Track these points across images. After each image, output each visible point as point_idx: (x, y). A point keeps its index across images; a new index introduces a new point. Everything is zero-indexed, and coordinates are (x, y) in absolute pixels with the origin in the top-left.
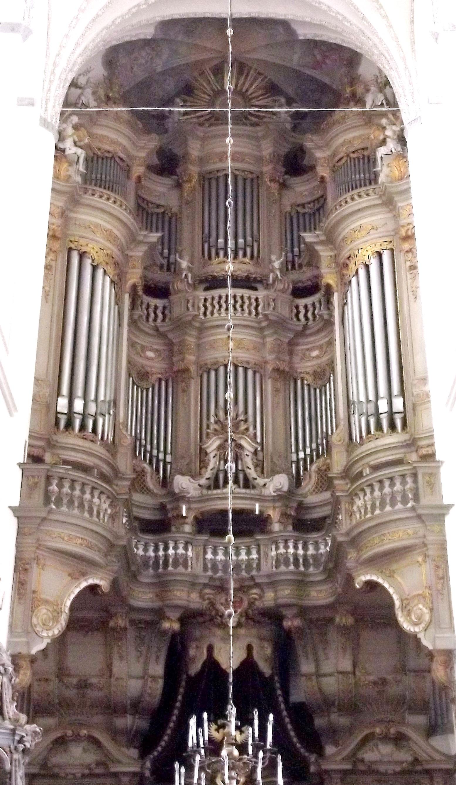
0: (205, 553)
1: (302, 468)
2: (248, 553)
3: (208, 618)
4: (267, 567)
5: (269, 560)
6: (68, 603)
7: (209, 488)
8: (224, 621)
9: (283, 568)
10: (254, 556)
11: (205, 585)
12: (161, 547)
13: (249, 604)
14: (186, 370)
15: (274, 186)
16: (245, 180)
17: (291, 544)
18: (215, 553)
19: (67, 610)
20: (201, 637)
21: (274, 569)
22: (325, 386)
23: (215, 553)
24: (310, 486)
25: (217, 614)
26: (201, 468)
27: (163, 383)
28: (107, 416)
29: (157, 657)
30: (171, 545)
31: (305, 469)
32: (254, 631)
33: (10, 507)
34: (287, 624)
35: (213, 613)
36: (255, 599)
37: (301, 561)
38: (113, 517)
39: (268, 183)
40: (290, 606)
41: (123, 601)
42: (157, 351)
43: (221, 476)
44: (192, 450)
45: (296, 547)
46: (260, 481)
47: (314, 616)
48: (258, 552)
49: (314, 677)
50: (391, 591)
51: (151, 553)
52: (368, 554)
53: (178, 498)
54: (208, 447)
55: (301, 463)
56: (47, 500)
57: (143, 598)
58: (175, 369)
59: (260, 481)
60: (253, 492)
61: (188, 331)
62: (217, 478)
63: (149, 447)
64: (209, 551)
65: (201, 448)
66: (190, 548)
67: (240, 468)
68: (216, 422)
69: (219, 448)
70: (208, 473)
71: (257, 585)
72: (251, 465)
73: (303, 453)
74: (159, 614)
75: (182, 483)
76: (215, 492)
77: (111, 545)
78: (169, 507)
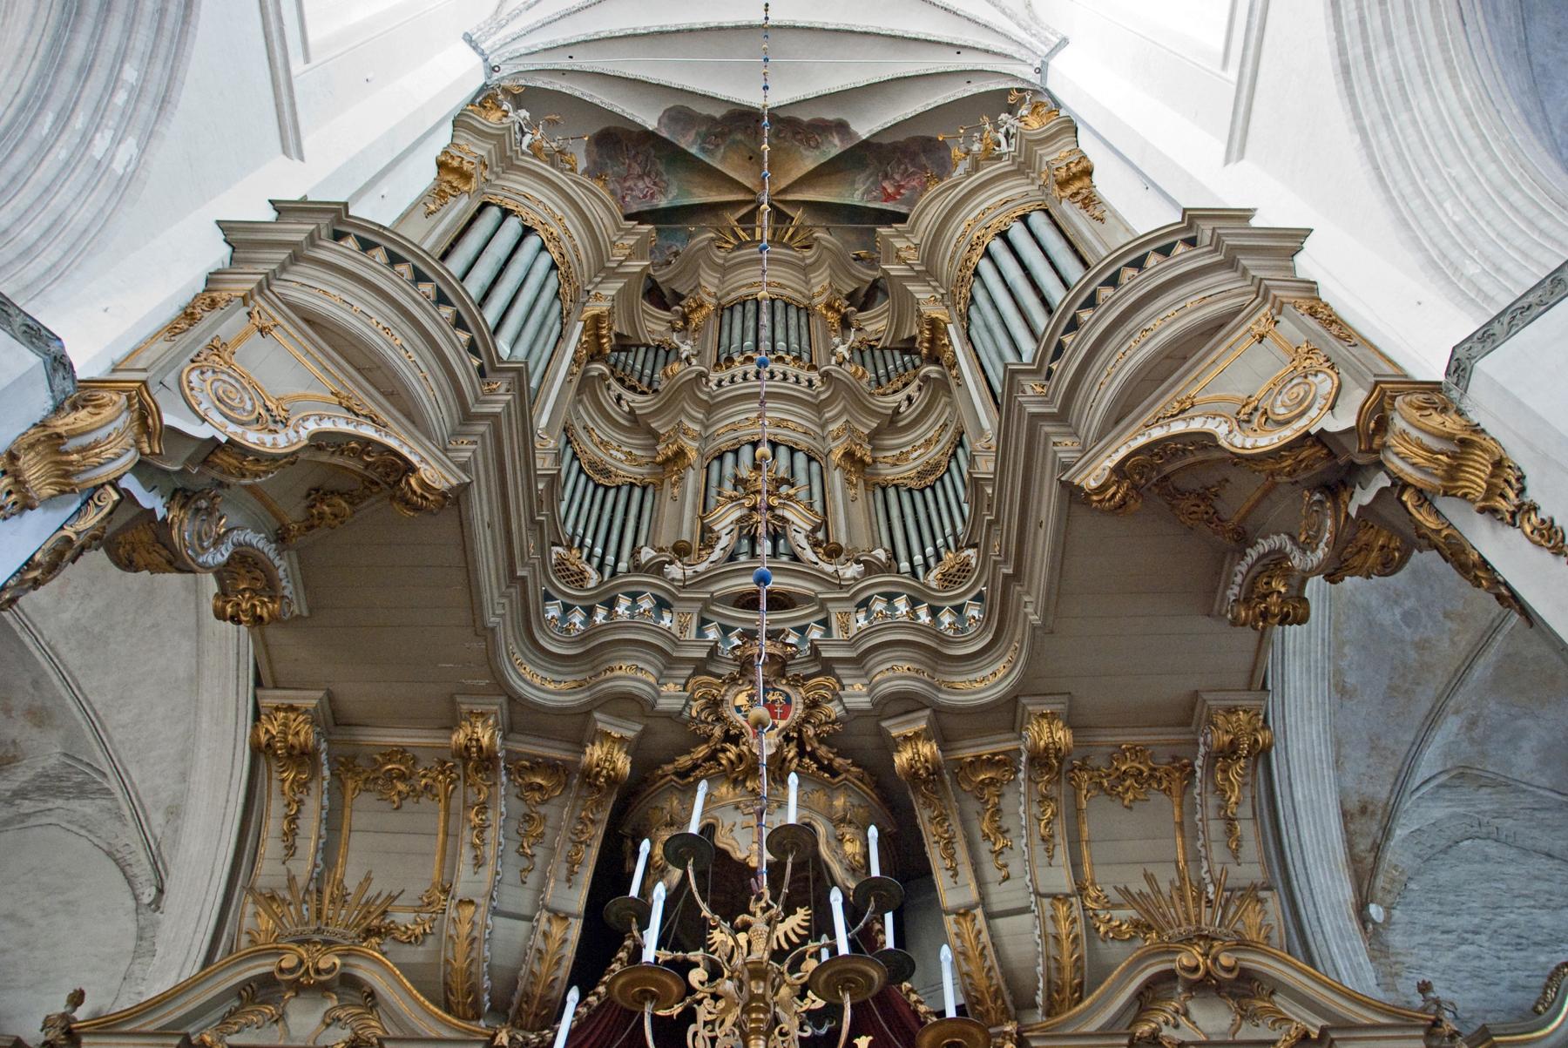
3: (702, 751)
6: (312, 426)
8: (745, 748)
11: (701, 667)
13: (807, 707)
14: (680, 454)
16: (787, 305)
19: (304, 434)
22: (941, 479)
27: (637, 493)
29: (573, 864)
33: (218, 222)
34: (902, 759)
35: (718, 731)
47: (967, 754)
49: (979, 912)
67: (782, 549)
71: (827, 667)
77: (467, 417)
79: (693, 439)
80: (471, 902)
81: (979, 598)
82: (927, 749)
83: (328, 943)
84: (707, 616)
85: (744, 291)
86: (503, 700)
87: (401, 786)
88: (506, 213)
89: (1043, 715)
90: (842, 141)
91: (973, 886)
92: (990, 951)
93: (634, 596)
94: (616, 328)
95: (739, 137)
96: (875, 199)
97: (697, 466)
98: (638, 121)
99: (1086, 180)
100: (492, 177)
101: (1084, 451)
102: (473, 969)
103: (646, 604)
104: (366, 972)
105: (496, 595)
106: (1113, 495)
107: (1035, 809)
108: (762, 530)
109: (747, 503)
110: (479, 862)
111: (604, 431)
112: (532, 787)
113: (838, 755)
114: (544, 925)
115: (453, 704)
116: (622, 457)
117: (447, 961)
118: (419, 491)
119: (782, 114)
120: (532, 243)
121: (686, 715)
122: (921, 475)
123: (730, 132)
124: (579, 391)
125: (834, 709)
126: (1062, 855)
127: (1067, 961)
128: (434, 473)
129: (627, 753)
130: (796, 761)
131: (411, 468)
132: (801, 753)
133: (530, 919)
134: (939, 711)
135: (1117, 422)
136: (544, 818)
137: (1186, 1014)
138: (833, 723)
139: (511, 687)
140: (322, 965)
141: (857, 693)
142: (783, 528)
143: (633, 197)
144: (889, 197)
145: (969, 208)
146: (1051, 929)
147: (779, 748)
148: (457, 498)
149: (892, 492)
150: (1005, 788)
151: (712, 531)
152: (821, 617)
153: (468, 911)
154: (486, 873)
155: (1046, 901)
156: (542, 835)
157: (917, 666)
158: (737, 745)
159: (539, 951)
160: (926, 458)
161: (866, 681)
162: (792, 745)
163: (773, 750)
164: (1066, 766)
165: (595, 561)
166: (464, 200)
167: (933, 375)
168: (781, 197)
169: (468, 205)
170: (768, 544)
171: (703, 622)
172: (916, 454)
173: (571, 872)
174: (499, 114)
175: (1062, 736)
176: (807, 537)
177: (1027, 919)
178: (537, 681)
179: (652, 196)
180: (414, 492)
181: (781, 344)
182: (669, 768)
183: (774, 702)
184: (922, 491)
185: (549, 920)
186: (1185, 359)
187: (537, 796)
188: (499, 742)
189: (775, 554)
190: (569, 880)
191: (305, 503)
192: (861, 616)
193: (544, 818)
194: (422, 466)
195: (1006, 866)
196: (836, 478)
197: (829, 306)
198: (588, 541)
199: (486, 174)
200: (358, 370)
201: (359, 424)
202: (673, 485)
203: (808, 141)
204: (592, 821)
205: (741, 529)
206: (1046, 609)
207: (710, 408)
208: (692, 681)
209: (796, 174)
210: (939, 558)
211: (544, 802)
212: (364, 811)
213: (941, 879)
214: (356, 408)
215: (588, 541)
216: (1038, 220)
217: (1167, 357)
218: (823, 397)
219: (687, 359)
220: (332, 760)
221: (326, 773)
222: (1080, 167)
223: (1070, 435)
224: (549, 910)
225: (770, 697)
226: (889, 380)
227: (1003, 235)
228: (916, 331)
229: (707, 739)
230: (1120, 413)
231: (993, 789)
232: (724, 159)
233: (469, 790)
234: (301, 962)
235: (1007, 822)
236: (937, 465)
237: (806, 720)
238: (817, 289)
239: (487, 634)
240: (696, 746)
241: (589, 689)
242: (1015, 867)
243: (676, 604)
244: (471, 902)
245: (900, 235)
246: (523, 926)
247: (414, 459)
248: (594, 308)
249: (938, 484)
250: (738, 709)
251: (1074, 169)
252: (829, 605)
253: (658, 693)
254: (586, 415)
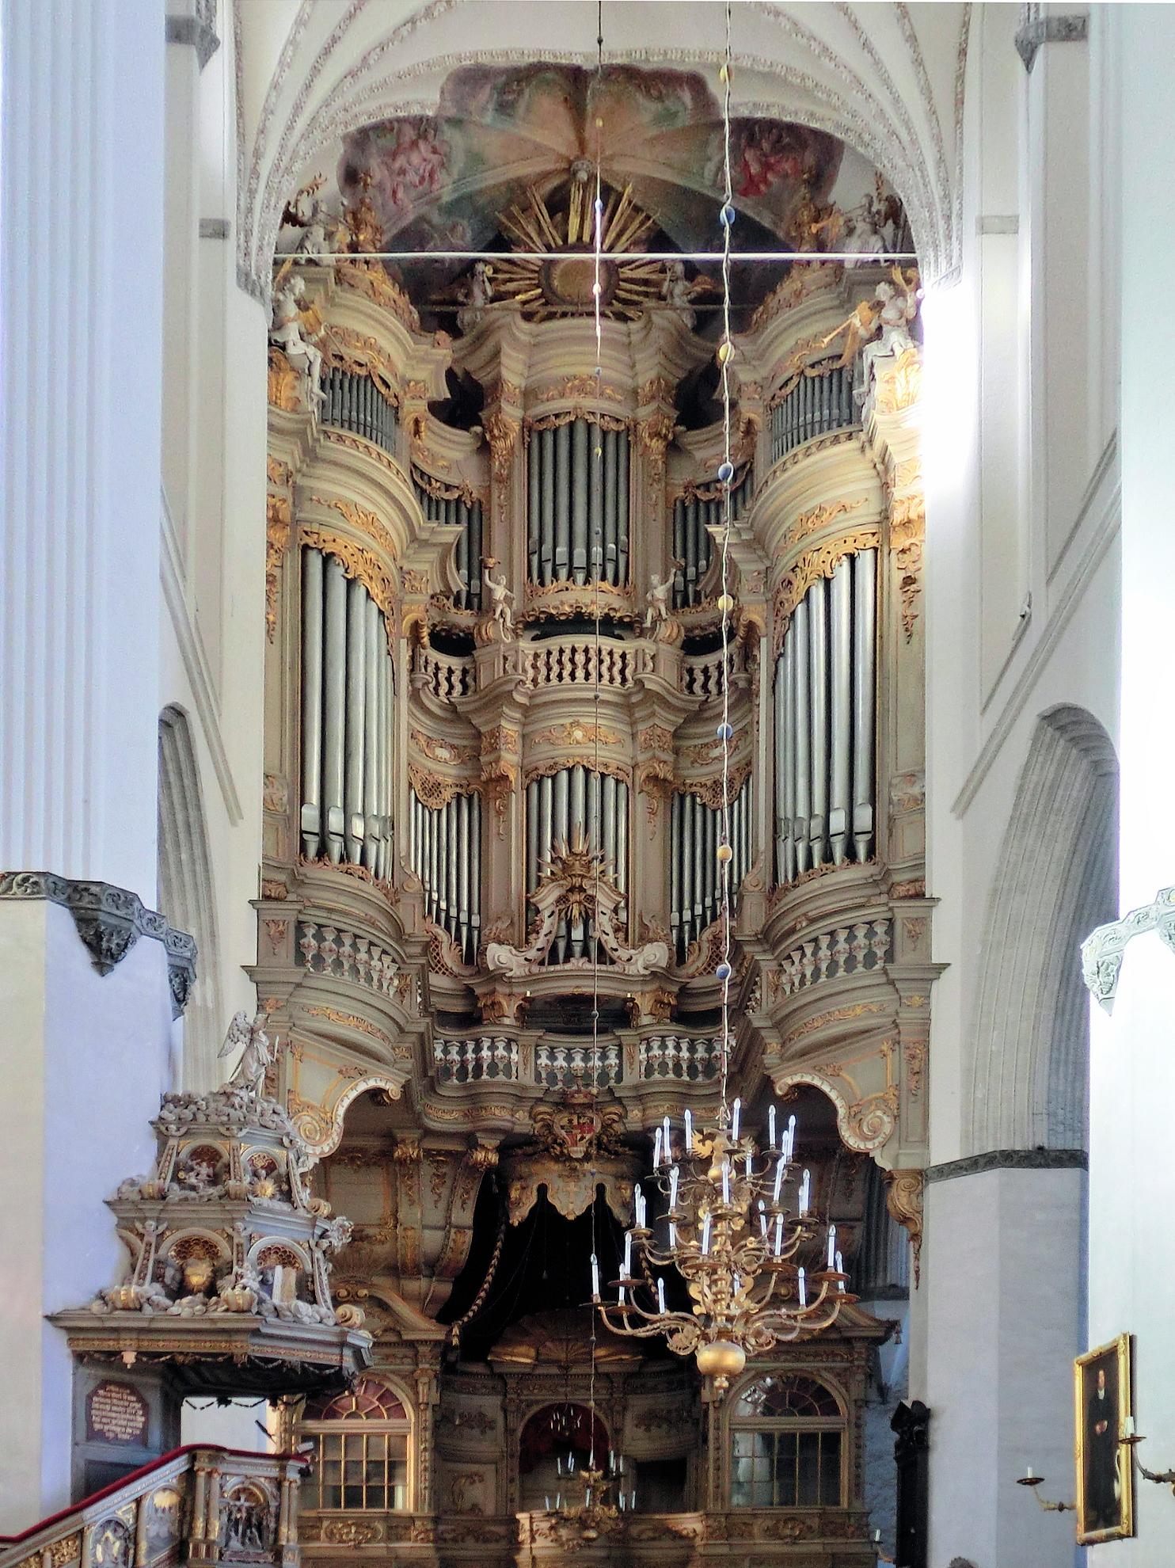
0: (537, 1056)
1: (686, 936)
2: (604, 1057)
3: (541, 1147)
4: (631, 1077)
5: (636, 1066)
7: (542, 963)
9: (657, 1076)
10: (613, 1060)
12: (471, 1046)
17: (670, 1044)
18: (552, 1057)
20: (531, 1175)
21: (643, 1079)
23: (552, 1057)
24: (699, 964)
25: (555, 1142)
26: (528, 934)
28: (383, 842)
30: (486, 1043)
31: (693, 938)
32: (611, 1168)
36: (614, 1121)
37: (685, 1067)
38: (401, 992)
41: (417, 1122)
43: (562, 944)
45: (678, 1048)
46: (623, 954)
48: (620, 1056)
50: (833, 1095)
51: (455, 1056)
52: (799, 1044)
53: (497, 977)
54: (542, 901)
55: (687, 927)
56: (300, 958)
57: (445, 1116)
59: (623, 954)
60: (611, 968)
62: (554, 948)
64: (544, 1054)
65: (528, 900)
66: (514, 1048)
68: (553, 861)
69: (559, 900)
70: (540, 941)
71: (619, 1101)
72: (609, 930)
74: (470, 1140)
75: (498, 955)
76: (552, 968)
78: (478, 991)
84: (540, 1042)
108: (576, 912)
182: (520, 1152)
205: (560, 911)
250: (562, 1127)
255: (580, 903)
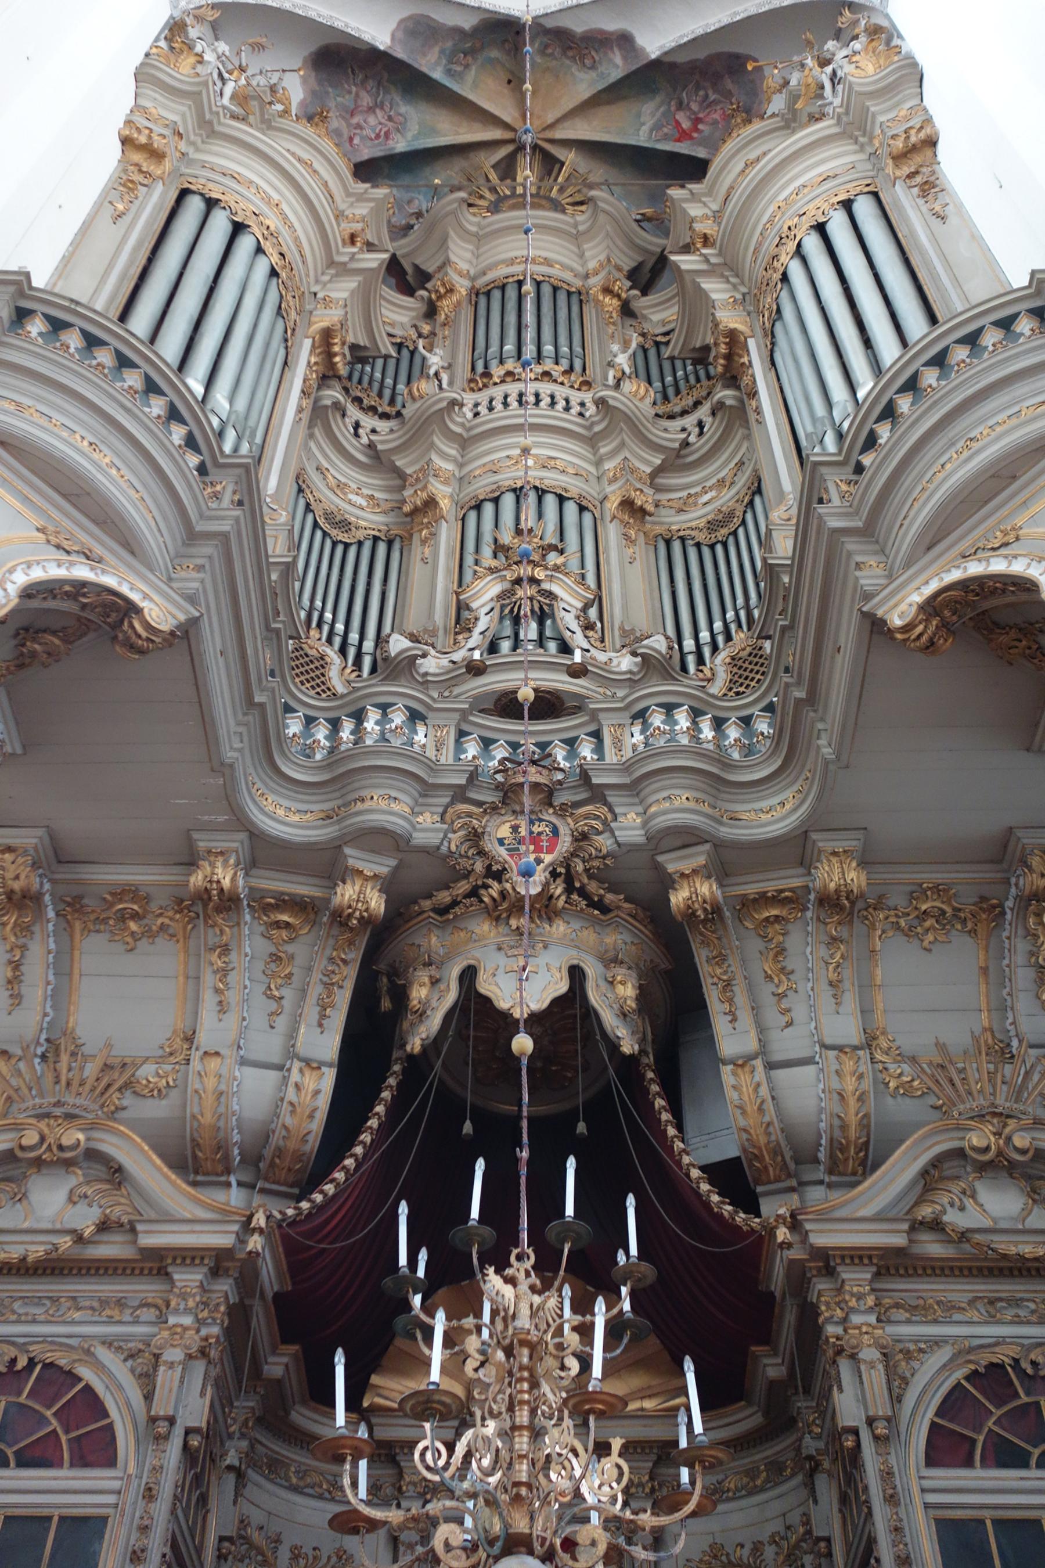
3: (463, 887)
6: (20, 579)
8: (508, 886)
11: (459, 794)
14: (431, 503)
15: (611, 304)
16: (555, 289)
19: (13, 590)
22: (735, 533)
27: (382, 548)
29: (324, 1008)
32: (589, 936)
34: (678, 898)
35: (479, 867)
39: (601, 297)
40: (686, 838)
42: (372, 497)
44: (439, 617)
47: (751, 889)
49: (758, 1063)
58: (407, 508)
61: (435, 439)
63: (340, 627)
67: (548, 633)
71: (598, 794)
73: (692, 642)
79: (446, 482)
80: (217, 1054)
81: (770, 708)
82: (706, 889)
83: (70, 1117)
84: (466, 727)
85: (502, 271)
86: (243, 836)
87: (133, 926)
88: (211, 203)
89: (835, 854)
90: (625, 58)
91: (753, 1034)
92: (769, 1105)
93: (384, 708)
94: (350, 339)
95: (495, 53)
96: (666, 138)
97: (451, 518)
98: (366, 37)
99: (929, 152)
100: (191, 151)
101: (891, 577)
102: (221, 1124)
103: (398, 718)
104: (111, 1146)
105: (232, 722)
106: (920, 635)
107: (823, 952)
109: (509, 575)
110: (222, 1008)
111: (342, 471)
112: (278, 925)
113: (609, 890)
114: (295, 1076)
115: (191, 844)
116: (360, 502)
117: (193, 1117)
118: (144, 634)
119: (549, 24)
120: (245, 244)
121: (444, 849)
122: (712, 526)
123: (482, 48)
124: (311, 426)
125: (604, 842)
126: (850, 1001)
127: (853, 1120)
128: (158, 610)
129: (380, 891)
130: (563, 898)
131: (131, 609)
132: (569, 889)
133: (280, 1068)
134: (719, 846)
135: (929, 549)
136: (291, 957)
137: (973, 1196)
138: (604, 857)
139: (253, 823)
140: (66, 1141)
141: (630, 825)
142: (551, 606)
143: (362, 138)
144: (683, 136)
145: (782, 178)
146: (835, 1084)
147: (546, 885)
148: (187, 632)
149: (677, 546)
150: (790, 927)
151: (468, 608)
152: (592, 728)
153: (213, 1064)
154: (231, 1020)
155: (832, 1054)
156: (289, 976)
157: (699, 795)
158: (500, 882)
159: (291, 1104)
160: (716, 504)
161: (640, 809)
162: (559, 881)
163: (539, 889)
164: (860, 905)
165: (337, 641)
166: (159, 188)
167: (729, 402)
168: (549, 135)
169: (164, 194)
170: (534, 625)
171: (462, 734)
172: (706, 498)
173: (323, 1016)
174: (192, 60)
175: (855, 877)
176: (578, 617)
177: (809, 1071)
178: (281, 812)
179: (387, 135)
180: (139, 637)
181: (548, 349)
182: (427, 904)
183: (540, 834)
184: (712, 547)
185: (301, 1071)
186: (1014, 478)
187: (284, 934)
188: (241, 882)
189: (541, 642)
190: (320, 1025)
191: (14, 642)
192: (637, 729)
193: (291, 957)
194: (144, 604)
195: (789, 1010)
196: (612, 533)
197: (607, 290)
198: (328, 616)
199: (183, 146)
200: (64, 496)
201: (72, 564)
202: (424, 542)
203: (582, 58)
204: (344, 961)
205: (503, 607)
206: (840, 744)
207: (464, 443)
208: (450, 810)
209: (568, 103)
210: (729, 638)
211: (292, 940)
212: (95, 951)
213: (720, 1024)
214: (66, 544)
215: (328, 616)
216: (864, 208)
217: (993, 476)
218: (597, 429)
219: (437, 374)
220: (57, 899)
221: (51, 914)
222: (922, 135)
223: (876, 553)
224: (300, 1059)
225: (536, 829)
226: (678, 392)
227: (821, 228)
228: (710, 340)
229: (468, 874)
230: (935, 537)
231: (777, 927)
232: (475, 85)
233: (210, 931)
234: (43, 1139)
235: (790, 964)
236: (731, 515)
237: (573, 855)
238: (592, 265)
239: (223, 769)
240: (457, 881)
241: (339, 822)
242: (800, 1013)
243: (430, 715)
244: (217, 1054)
245: (694, 197)
246: (273, 1075)
247: (135, 597)
248: (325, 318)
249: (731, 540)
250: (501, 842)
251: (913, 139)
252: (602, 716)
253: (414, 827)
254: (322, 452)
255: (531, 599)
